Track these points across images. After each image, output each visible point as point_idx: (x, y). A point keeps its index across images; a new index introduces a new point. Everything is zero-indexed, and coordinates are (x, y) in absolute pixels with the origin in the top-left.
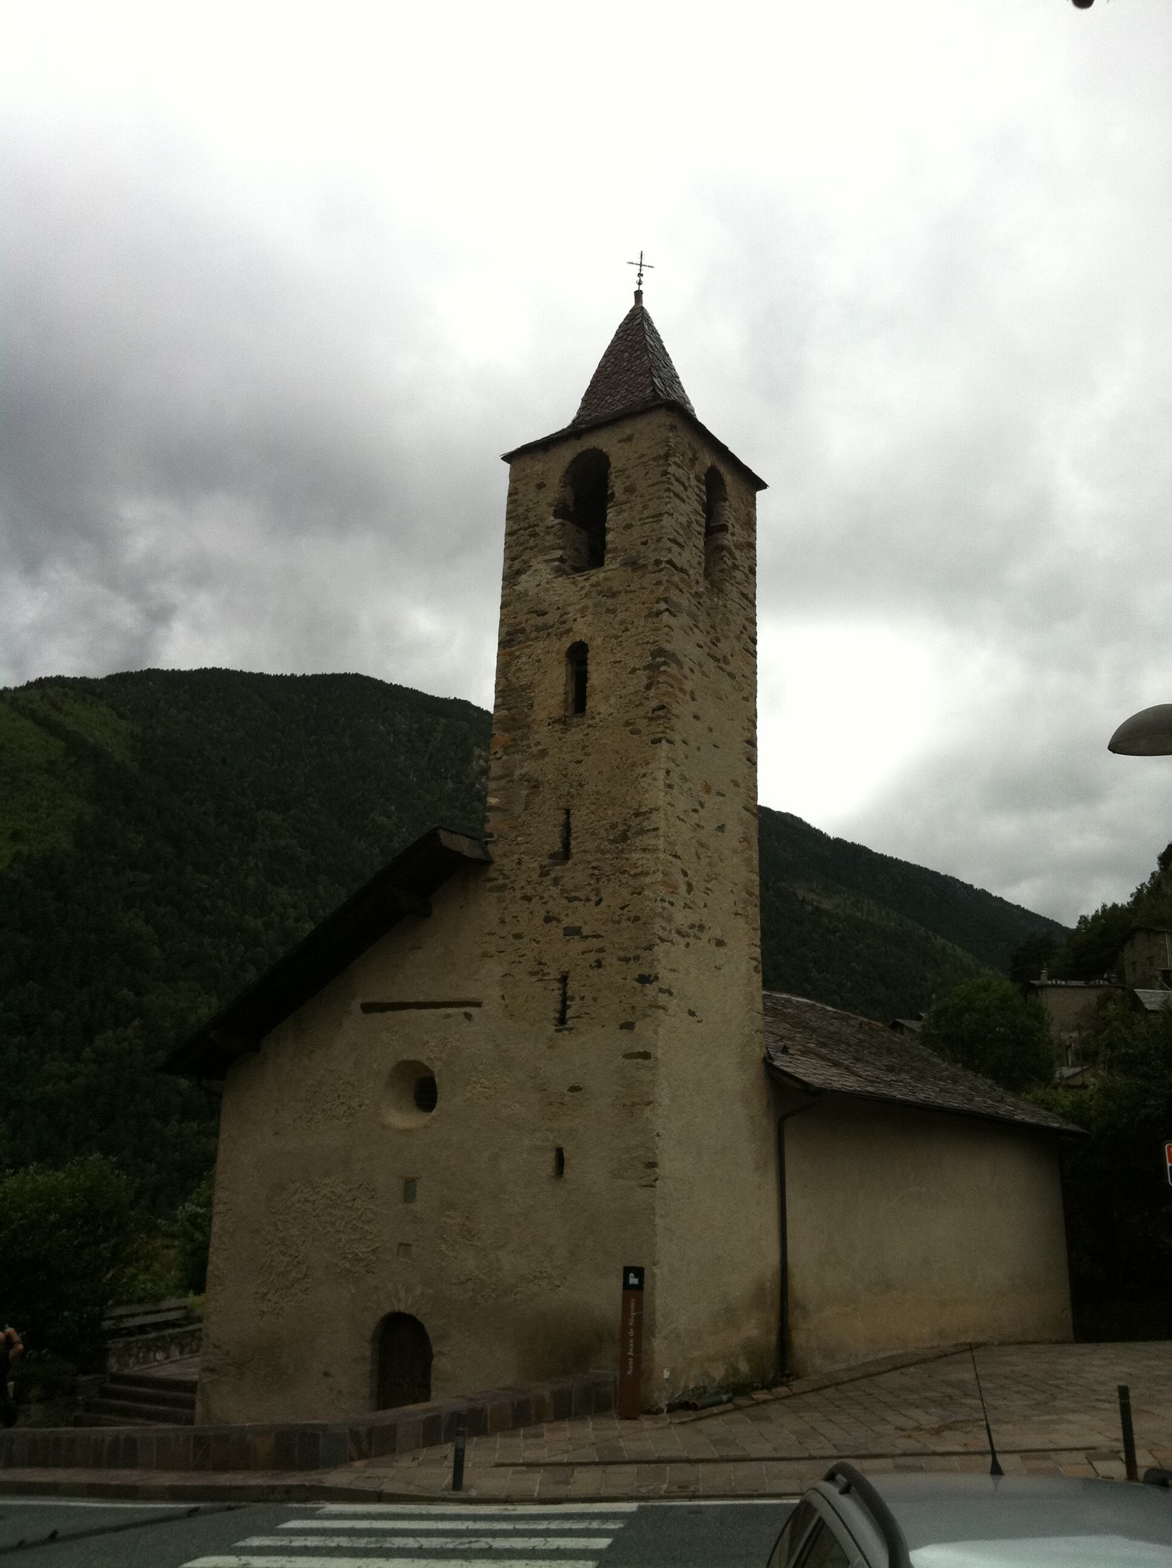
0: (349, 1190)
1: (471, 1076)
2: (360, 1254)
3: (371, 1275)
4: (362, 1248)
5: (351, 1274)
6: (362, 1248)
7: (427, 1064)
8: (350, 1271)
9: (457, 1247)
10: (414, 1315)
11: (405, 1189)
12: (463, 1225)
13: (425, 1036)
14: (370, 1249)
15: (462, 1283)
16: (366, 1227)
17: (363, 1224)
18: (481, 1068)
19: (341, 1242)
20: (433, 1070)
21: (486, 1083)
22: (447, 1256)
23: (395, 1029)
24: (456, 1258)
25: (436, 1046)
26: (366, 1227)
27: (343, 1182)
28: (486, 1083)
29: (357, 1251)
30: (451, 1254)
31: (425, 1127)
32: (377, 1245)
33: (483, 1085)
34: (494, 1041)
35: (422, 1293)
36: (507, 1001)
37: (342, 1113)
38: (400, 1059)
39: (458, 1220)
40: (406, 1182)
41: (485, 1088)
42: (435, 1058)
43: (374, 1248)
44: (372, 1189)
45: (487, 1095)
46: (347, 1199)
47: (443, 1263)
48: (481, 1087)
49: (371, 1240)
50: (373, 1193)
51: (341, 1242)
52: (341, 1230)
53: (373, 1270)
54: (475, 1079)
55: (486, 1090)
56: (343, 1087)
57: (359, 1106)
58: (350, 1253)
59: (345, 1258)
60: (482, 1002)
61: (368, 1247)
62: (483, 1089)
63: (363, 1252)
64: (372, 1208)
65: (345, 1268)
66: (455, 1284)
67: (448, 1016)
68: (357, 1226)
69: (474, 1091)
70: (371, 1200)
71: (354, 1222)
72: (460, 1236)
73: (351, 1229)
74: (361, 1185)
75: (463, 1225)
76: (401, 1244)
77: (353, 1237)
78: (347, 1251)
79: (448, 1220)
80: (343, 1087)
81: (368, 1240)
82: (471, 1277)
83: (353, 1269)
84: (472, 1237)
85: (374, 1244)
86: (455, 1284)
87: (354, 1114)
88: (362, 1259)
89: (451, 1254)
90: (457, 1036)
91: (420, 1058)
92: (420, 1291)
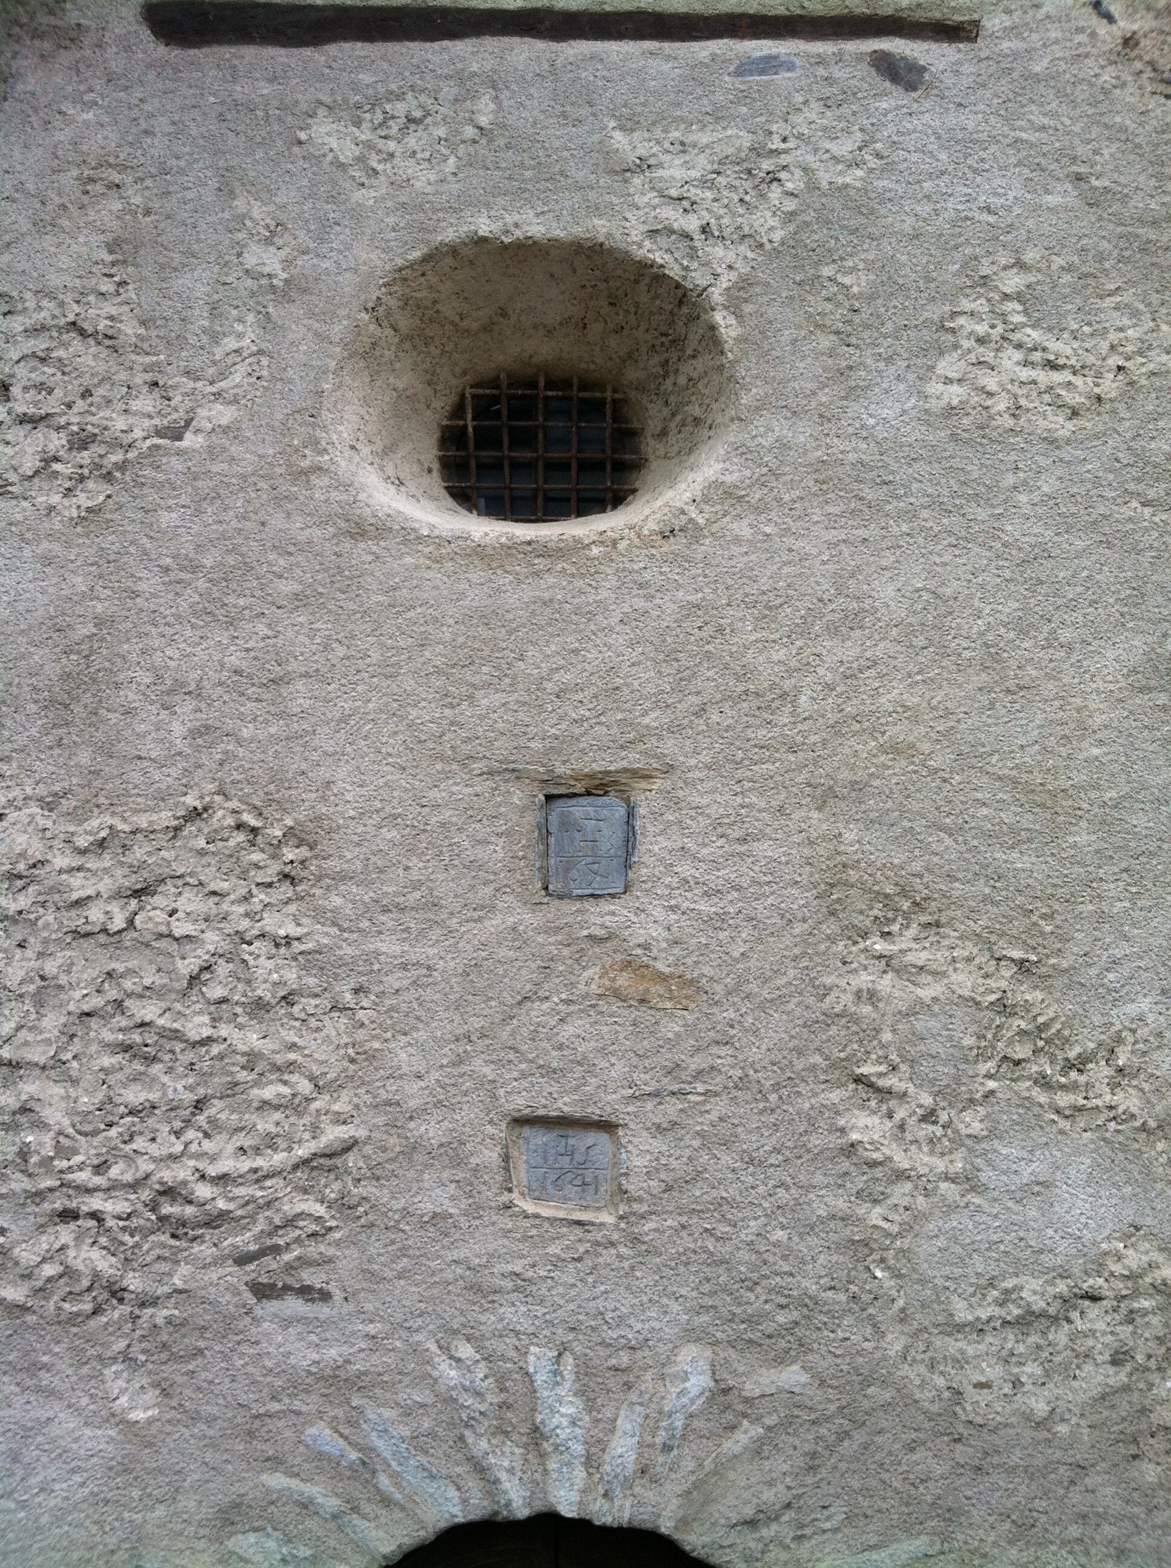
0: (102, 844)
1: (954, 315)
2: (203, 1191)
3: (293, 1305)
4: (213, 1158)
5: (117, 1312)
6: (213, 1158)
7: (658, 257)
8: (117, 1293)
9: (972, 1122)
10: (665, 1527)
11: (545, 832)
12: (1002, 1007)
13: (619, 139)
14: (278, 1159)
15: (1027, 1320)
16: (250, 1039)
17: (215, 1021)
18: (1013, 282)
19: (40, 1125)
20: (699, 278)
21: (1060, 347)
22: (901, 1175)
23: (400, 108)
24: (969, 1182)
25: (704, 183)
26: (250, 1039)
27: (49, 805)
28: (1054, 346)
29: (169, 1175)
30: (925, 1161)
31: (668, 534)
32: (334, 1134)
33: (1037, 356)
34: (1079, 178)
35: (721, 1393)
36: (1125, 25)
37: (29, 465)
38: (449, 234)
39: (964, 981)
40: (549, 798)
41: (1053, 366)
42: (705, 229)
43: (302, 1152)
44: (289, 832)
45: (1074, 399)
46: (79, 886)
47: (875, 1215)
48: (1026, 363)
49: (294, 1105)
50: (289, 854)
51: (40, 1125)
52: (39, 1055)
53: (309, 1277)
54: (981, 329)
55: (1058, 377)
56: (39, 344)
57: (159, 433)
58: (109, 1190)
59: (68, 1215)
60: (976, 24)
61: (270, 1142)
62: (1044, 377)
63: (223, 1179)
64: (291, 929)
65: (68, 1273)
66: (979, 1329)
67: (769, 65)
68: (176, 1035)
69: (991, 382)
70: (286, 890)
71: (148, 1011)
72: (990, 1066)
73: (126, 1048)
74: (195, 814)
75: (1002, 1007)
76: (521, 1122)
77: (135, 1095)
78: (83, 1177)
79: (886, 984)
80: (39, 344)
81: (264, 1105)
82: (1096, 1282)
83: (134, 1282)
84: (1069, 1066)
85: (315, 1130)
86: (979, 1329)
87: (122, 466)
88: (216, 1220)
89: (925, 1161)
90: (844, 147)
91: (600, 228)
92: (699, 1382)
